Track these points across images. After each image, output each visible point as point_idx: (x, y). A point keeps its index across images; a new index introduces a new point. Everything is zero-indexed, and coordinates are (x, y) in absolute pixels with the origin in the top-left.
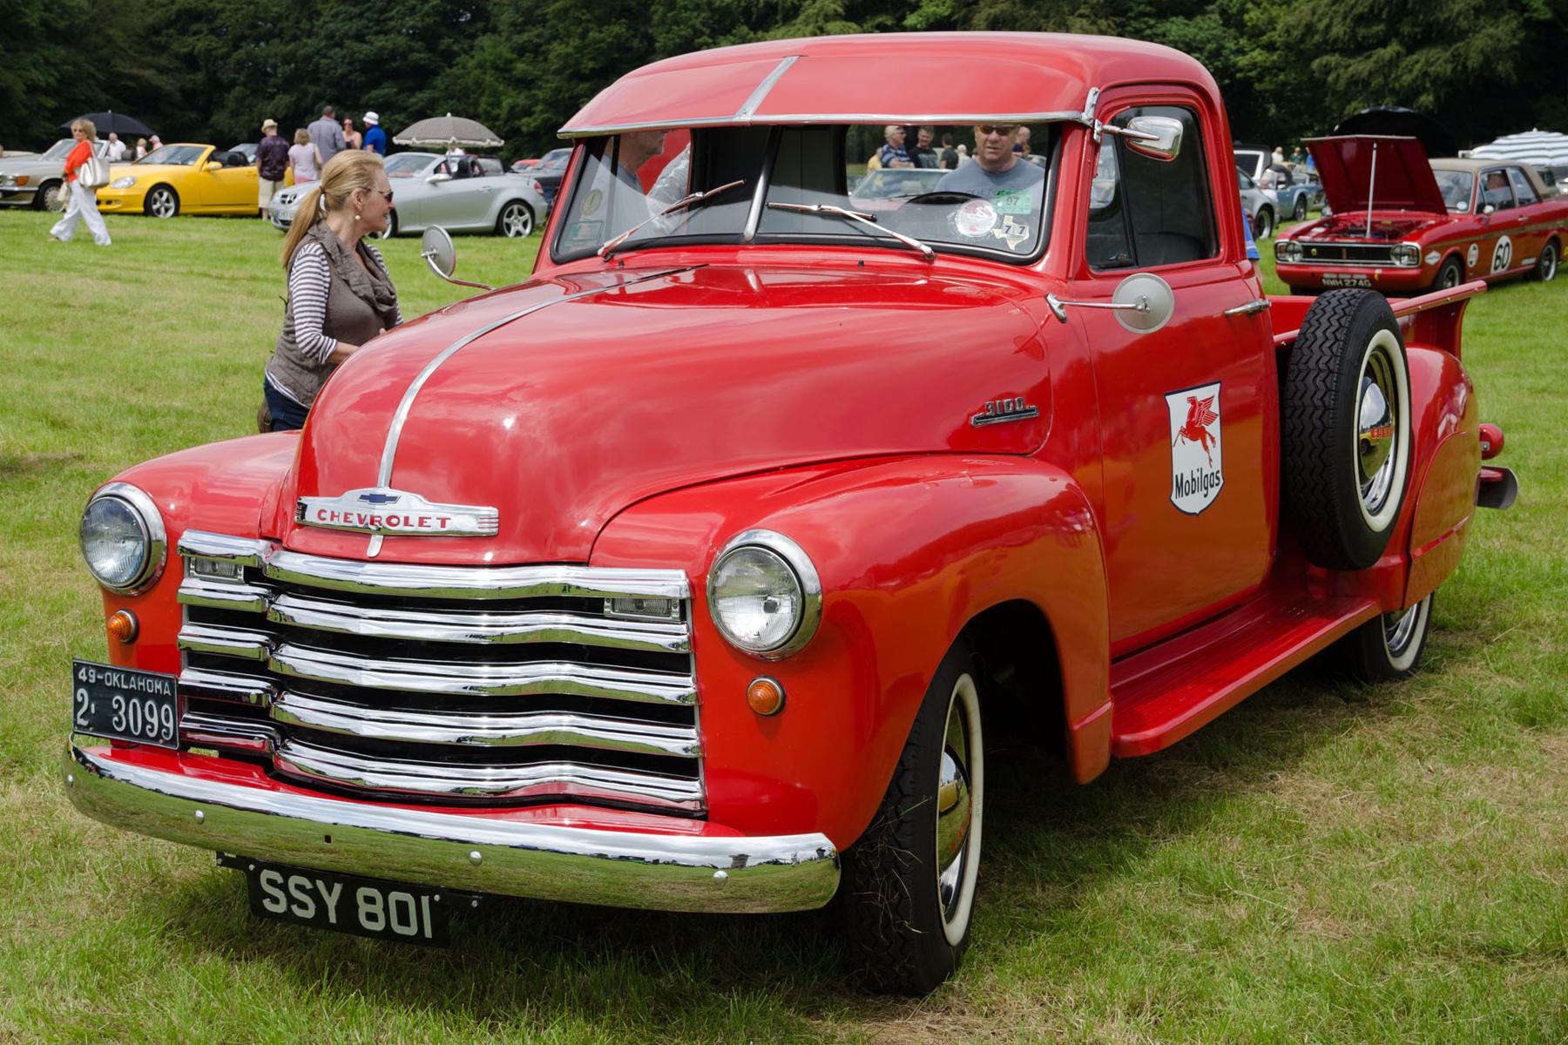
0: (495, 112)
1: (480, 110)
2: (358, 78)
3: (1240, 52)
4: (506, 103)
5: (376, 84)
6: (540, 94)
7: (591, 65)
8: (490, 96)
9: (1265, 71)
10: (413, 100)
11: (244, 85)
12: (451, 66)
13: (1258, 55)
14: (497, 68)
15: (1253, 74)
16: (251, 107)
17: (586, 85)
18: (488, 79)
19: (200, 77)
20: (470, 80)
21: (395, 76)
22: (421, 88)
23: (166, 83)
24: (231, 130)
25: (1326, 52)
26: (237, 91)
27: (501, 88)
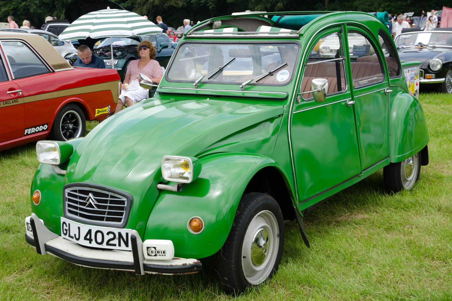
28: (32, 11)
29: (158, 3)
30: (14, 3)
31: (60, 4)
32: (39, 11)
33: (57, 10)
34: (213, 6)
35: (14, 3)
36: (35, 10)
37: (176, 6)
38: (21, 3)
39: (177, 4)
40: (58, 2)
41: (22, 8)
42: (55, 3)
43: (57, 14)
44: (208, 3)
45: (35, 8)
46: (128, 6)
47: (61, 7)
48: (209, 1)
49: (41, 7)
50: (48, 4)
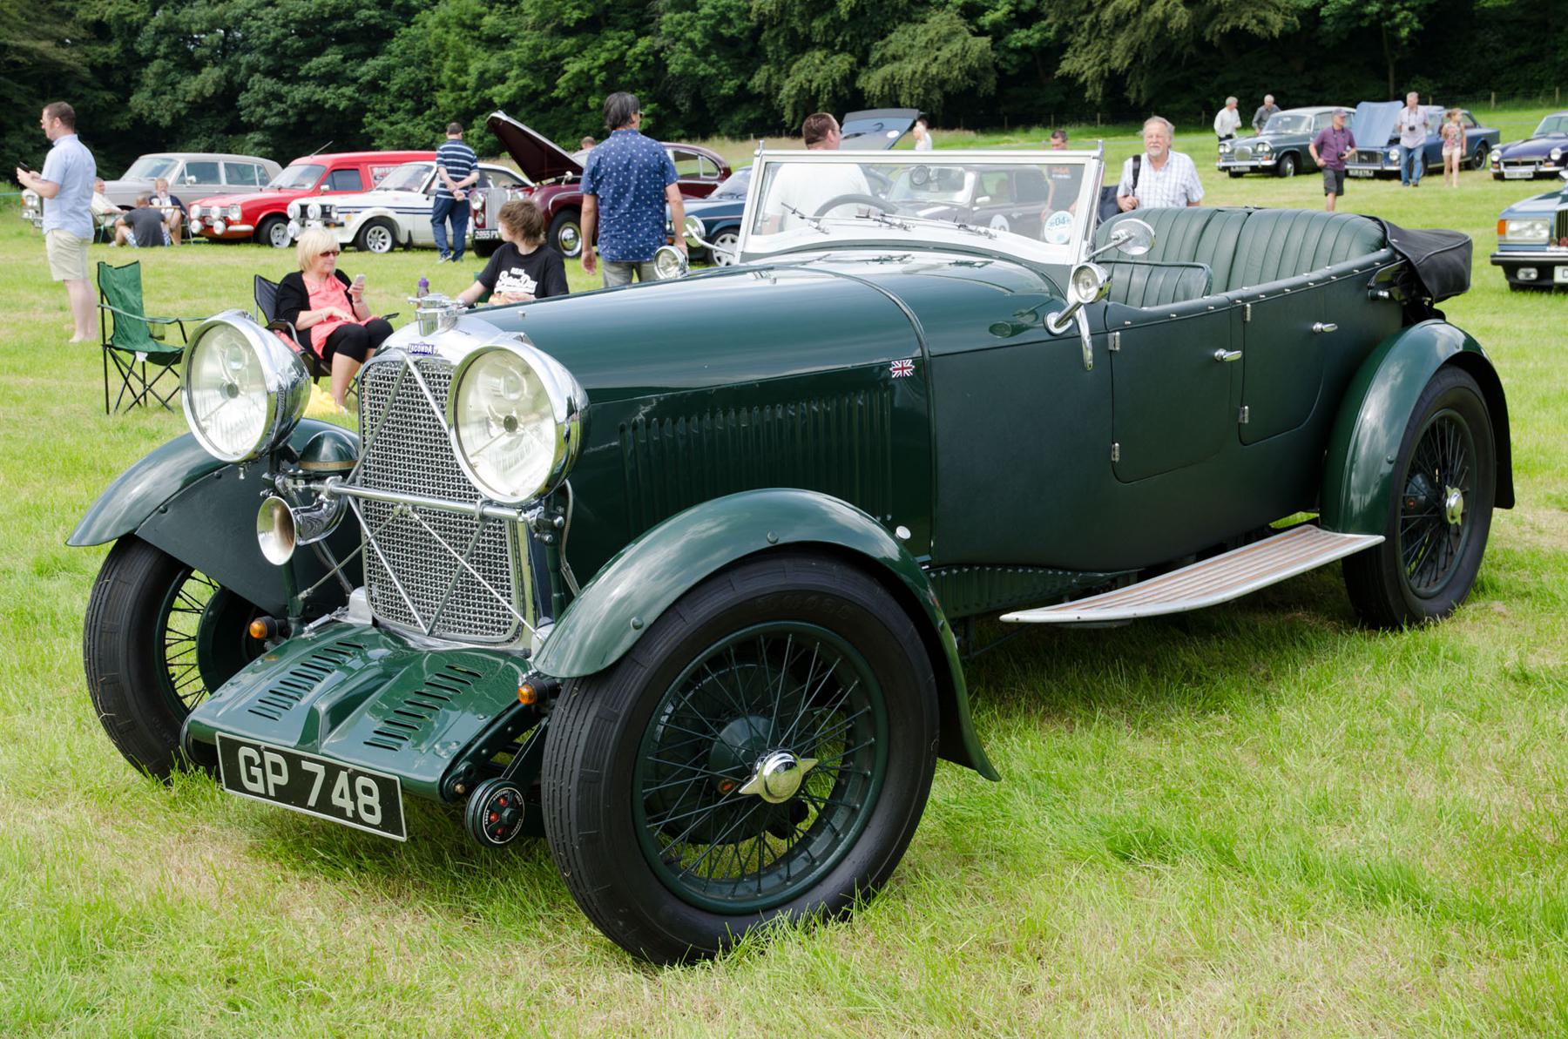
0: (461, 80)
1: (444, 79)
2: (295, 43)
4: (474, 67)
5: (318, 51)
7: (576, 14)
8: (455, 59)
10: (364, 69)
11: (166, 57)
12: (409, 25)
14: (463, 25)
16: (173, 84)
17: (572, 41)
18: (452, 38)
19: (114, 49)
21: (342, 38)
22: (373, 55)
23: (70, 57)
24: (151, 112)
26: (155, 66)
27: (469, 49)
28: (674, 68)
29: (1185, 23)
30: (609, 44)
31: (781, 41)
32: (702, 69)
33: (767, 61)
34: (1416, 25)
35: (609, 44)
36: (686, 65)
37: (1257, 30)
40: (773, 33)
41: (636, 60)
42: (764, 36)
43: (770, 77)
44: (1392, 16)
45: (687, 56)
46: (1047, 39)
48: (1397, 6)
49: (709, 54)
50: (733, 42)
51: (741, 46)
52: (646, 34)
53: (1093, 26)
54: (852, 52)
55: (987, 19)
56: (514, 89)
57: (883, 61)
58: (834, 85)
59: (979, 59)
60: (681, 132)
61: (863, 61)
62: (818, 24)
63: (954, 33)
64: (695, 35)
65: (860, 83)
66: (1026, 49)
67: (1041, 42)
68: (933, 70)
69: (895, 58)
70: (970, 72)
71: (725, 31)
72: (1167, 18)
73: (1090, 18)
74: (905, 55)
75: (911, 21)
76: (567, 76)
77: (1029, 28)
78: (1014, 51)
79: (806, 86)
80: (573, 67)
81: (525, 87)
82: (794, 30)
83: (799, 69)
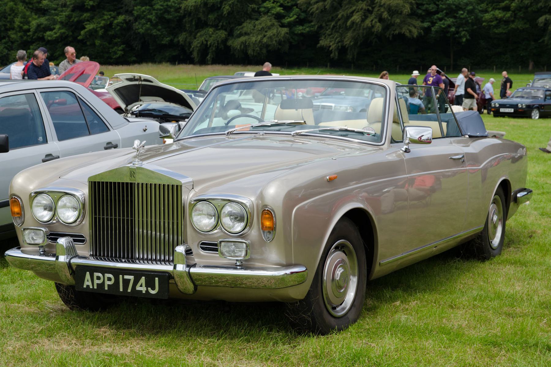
3: (486, 11)
6: (58, 18)
7: (91, 3)
9: (500, 21)
13: (499, 14)
15: (493, 23)
20: (7, 8)
25: (545, 13)
29: (380, 29)
31: (194, 23)
32: (154, 32)
33: (185, 31)
34: (468, 37)
36: (147, 30)
38: (115, 18)
39: (410, 31)
40: (190, 19)
45: (148, 26)
47: (194, 28)
48: (461, 29)
50: (168, 21)
51: (174, 22)
52: (119, 14)
53: (334, 26)
54: (226, 30)
55: (286, 21)
56: (58, 34)
57: (241, 35)
58: (218, 44)
59: (283, 37)
60: (134, 58)
61: (231, 34)
62: (211, 17)
63: (273, 25)
64: (152, 17)
65: (230, 43)
66: (302, 34)
67: (308, 32)
68: (265, 40)
69: (246, 34)
70: (280, 43)
71: (167, 16)
72: (373, 26)
73: (333, 24)
74: (251, 33)
75: (251, 18)
76: (86, 30)
77: (303, 25)
78: (297, 35)
79: (205, 43)
80: (90, 26)
81: (64, 33)
82: (199, 19)
83: (201, 36)
